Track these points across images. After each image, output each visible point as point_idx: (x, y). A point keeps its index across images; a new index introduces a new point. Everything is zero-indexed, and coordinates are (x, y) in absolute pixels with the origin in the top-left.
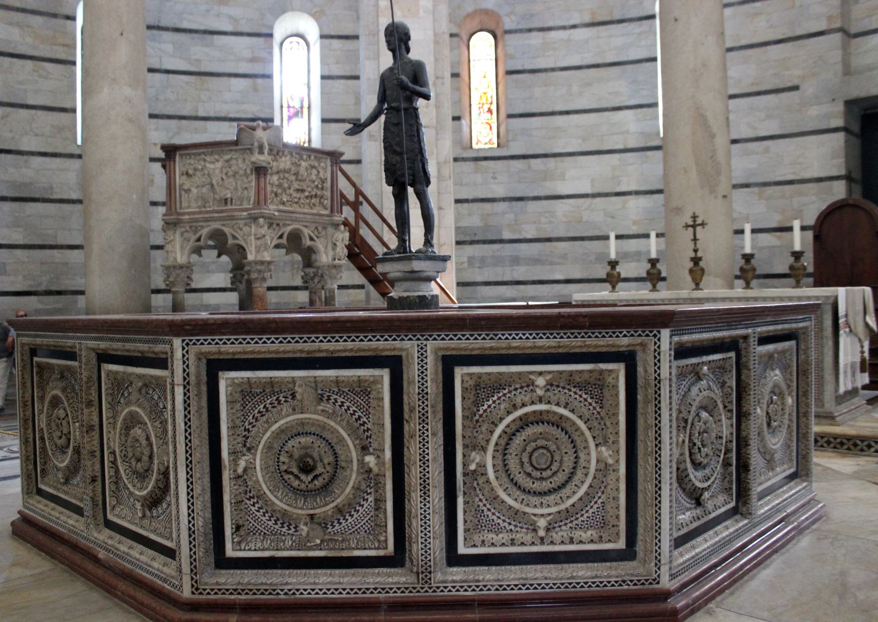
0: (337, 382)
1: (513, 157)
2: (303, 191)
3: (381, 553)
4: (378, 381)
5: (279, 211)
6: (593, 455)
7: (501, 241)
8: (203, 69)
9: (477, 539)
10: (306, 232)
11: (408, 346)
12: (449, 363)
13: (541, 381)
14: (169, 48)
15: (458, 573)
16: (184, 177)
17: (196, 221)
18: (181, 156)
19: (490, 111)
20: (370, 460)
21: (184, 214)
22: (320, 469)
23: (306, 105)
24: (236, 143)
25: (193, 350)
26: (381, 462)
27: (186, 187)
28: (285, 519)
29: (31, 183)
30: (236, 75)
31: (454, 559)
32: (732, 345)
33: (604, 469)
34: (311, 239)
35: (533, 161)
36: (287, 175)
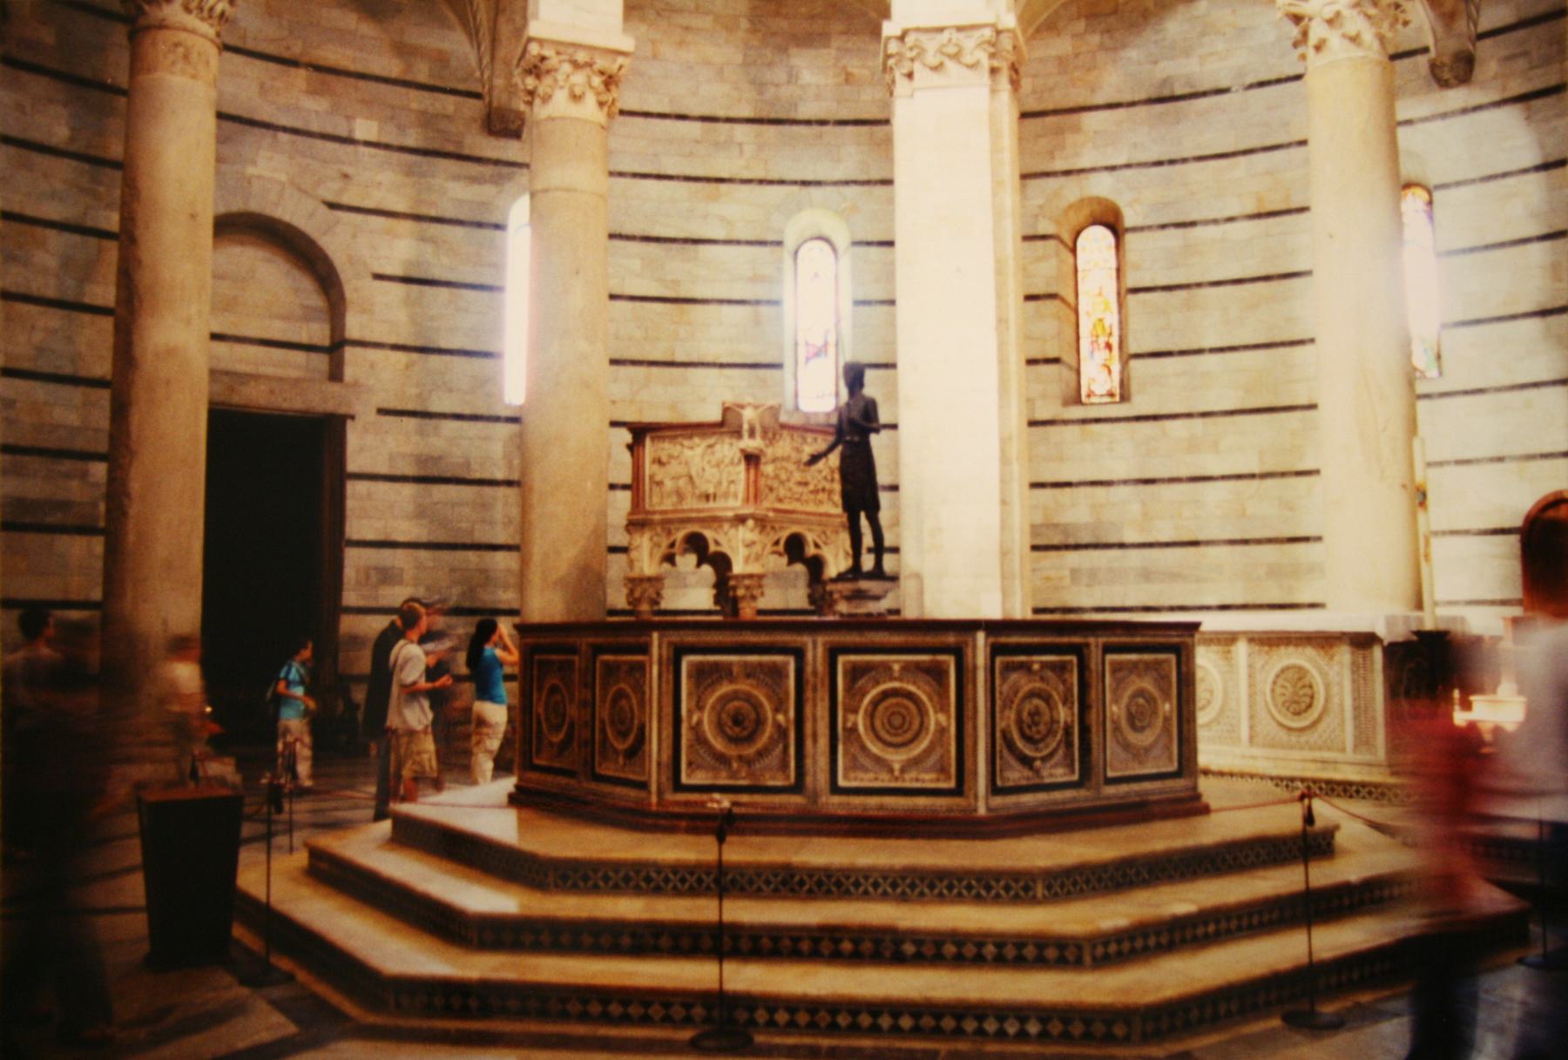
0: (760, 664)
1: (1138, 418)
2: (806, 484)
3: (786, 783)
4: (786, 664)
5: (776, 510)
6: (935, 719)
7: (1122, 546)
8: (683, 294)
9: (852, 775)
10: (810, 537)
11: (807, 640)
12: (833, 652)
13: (896, 667)
14: (636, 264)
15: (836, 799)
16: (656, 467)
17: (670, 521)
18: (653, 439)
19: (1109, 346)
20: (780, 718)
21: (654, 513)
22: (746, 723)
23: (832, 340)
24: (721, 424)
25: (665, 640)
26: (787, 720)
27: (658, 478)
28: (722, 759)
29: (440, 458)
30: (730, 302)
31: (835, 789)
32: (1079, 650)
33: (942, 731)
34: (817, 546)
35: (1168, 424)
36: (785, 464)
